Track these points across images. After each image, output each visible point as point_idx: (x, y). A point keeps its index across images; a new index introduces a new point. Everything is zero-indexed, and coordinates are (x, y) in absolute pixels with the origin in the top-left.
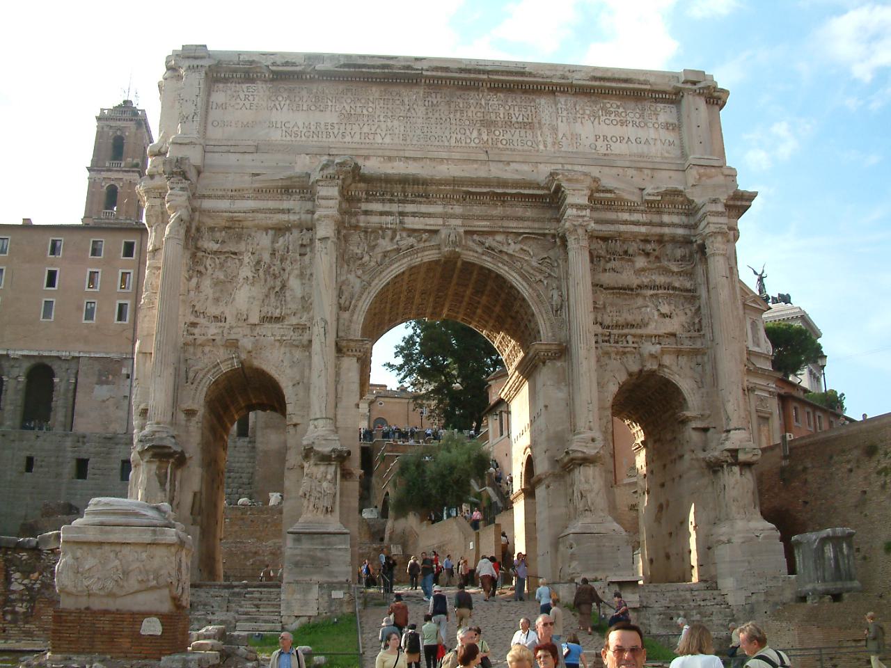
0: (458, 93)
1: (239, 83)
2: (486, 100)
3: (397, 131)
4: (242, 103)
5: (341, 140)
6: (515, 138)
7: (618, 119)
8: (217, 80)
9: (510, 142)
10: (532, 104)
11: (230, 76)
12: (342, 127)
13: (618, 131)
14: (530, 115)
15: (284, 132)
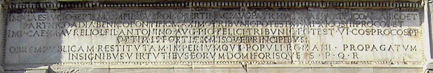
0: (222, 13)
1: (32, 12)
2: (246, 18)
3: (168, 51)
4: (34, 32)
5: (120, 60)
6: (271, 52)
7: (364, 28)
8: (12, 11)
9: (267, 55)
10: (287, 20)
11: (24, 7)
12: (121, 49)
13: (365, 40)
14: (285, 30)
15: (71, 55)
